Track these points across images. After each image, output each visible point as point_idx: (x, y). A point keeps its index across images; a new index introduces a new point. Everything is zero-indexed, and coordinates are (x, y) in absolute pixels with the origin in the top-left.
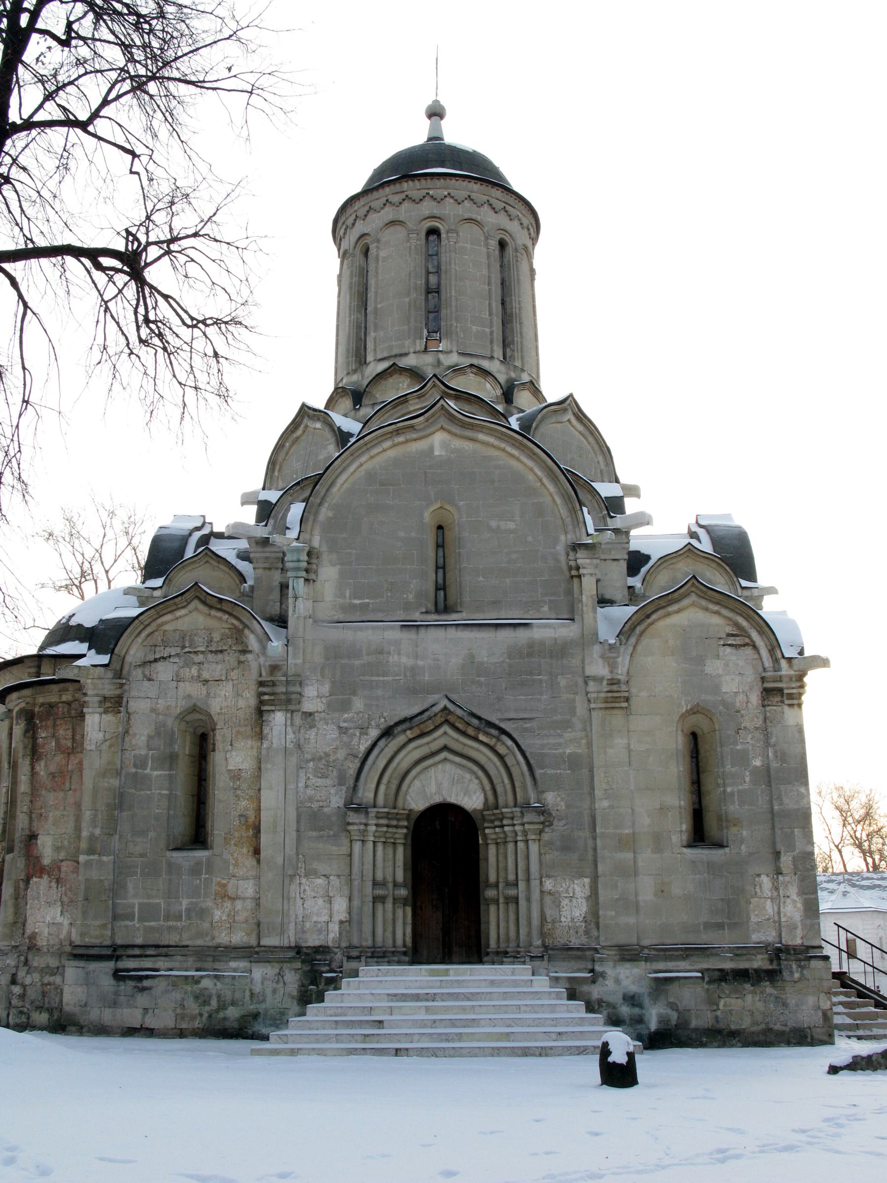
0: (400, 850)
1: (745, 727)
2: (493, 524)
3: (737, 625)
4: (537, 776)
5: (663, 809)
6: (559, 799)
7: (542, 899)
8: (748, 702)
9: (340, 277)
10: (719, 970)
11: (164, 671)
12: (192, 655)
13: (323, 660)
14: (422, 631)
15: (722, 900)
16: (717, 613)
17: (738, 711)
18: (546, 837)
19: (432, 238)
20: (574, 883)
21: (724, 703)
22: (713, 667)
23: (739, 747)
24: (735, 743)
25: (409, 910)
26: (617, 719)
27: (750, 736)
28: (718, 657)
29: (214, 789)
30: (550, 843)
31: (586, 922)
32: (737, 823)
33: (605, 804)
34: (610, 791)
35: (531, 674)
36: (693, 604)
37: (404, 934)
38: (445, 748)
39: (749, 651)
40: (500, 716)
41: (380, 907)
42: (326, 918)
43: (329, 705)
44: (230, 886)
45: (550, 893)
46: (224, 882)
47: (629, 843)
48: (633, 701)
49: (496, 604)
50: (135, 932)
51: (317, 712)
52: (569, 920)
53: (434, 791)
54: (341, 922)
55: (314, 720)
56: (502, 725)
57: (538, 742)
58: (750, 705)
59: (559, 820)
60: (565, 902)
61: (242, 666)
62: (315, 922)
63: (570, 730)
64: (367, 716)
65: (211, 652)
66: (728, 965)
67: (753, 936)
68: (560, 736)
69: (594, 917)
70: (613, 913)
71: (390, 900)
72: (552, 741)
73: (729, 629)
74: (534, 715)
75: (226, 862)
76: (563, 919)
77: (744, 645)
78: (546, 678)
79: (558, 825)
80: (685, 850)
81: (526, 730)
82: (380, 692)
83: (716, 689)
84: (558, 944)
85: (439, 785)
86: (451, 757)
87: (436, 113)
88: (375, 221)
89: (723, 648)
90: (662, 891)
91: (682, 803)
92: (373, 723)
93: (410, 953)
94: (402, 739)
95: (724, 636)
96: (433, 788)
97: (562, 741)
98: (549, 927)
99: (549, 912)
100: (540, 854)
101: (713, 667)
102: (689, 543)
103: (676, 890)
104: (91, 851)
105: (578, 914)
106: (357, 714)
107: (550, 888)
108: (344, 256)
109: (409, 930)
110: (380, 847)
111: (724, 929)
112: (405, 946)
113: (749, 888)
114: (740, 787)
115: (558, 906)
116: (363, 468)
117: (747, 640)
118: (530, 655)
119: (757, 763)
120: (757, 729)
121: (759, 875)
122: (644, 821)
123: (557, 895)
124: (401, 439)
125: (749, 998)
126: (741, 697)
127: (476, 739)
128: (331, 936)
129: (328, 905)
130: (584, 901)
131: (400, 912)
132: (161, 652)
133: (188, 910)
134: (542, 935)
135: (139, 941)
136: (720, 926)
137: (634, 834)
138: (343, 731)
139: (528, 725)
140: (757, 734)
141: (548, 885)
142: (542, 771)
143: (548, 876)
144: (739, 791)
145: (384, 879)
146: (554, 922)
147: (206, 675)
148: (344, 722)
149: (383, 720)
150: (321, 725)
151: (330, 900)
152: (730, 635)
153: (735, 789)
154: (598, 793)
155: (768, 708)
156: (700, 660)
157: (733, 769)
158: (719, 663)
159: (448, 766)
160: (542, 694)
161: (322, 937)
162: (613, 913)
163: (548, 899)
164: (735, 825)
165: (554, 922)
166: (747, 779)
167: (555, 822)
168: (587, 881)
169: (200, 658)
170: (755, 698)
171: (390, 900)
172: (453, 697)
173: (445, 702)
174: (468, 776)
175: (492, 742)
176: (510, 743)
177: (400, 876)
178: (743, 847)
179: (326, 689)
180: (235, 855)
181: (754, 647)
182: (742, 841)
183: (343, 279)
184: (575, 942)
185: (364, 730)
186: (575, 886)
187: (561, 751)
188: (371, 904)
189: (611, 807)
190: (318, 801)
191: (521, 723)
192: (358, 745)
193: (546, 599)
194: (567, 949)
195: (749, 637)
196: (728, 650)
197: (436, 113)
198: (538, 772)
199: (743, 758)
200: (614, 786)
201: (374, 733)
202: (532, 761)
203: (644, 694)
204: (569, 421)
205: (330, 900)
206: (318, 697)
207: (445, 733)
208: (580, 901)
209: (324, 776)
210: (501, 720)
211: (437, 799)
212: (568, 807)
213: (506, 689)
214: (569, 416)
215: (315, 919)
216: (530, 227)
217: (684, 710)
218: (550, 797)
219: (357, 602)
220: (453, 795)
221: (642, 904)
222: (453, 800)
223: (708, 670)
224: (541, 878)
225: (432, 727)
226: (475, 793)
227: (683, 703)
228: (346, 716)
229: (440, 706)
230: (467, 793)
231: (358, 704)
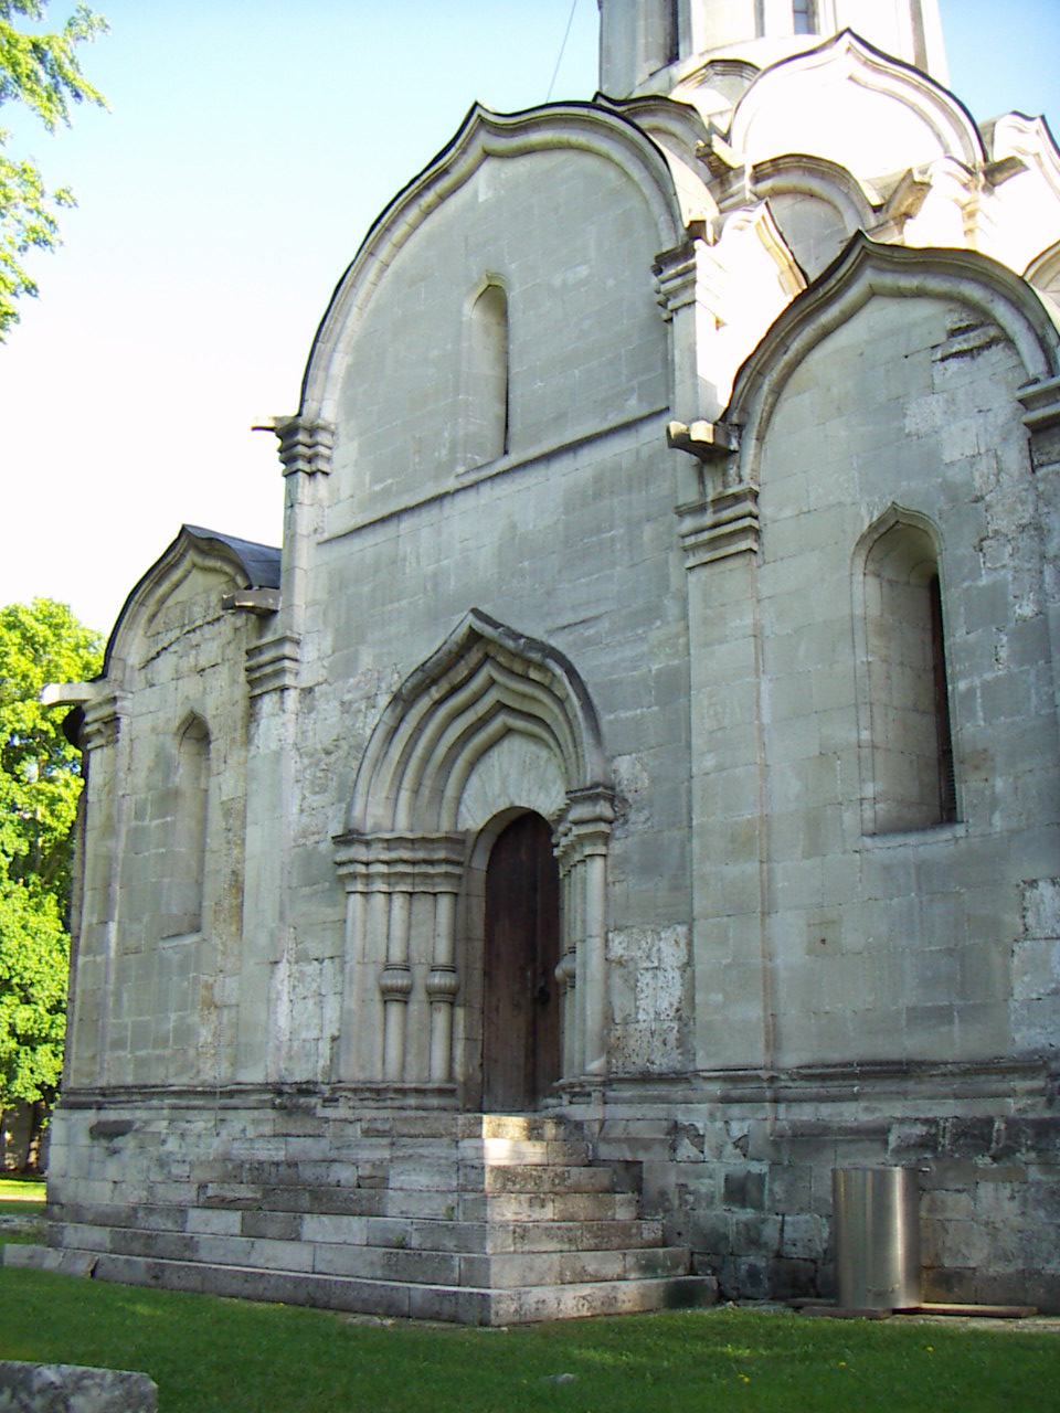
0: (445, 904)
1: (996, 532)
2: (557, 281)
3: (966, 303)
4: (604, 728)
5: (826, 756)
6: (638, 767)
7: (607, 976)
8: (1000, 471)
10: (927, 1121)
11: (165, 665)
12: (191, 635)
13: (327, 596)
14: (447, 502)
15: (950, 952)
16: (920, 294)
17: (978, 499)
18: (616, 847)
20: (660, 939)
21: (949, 490)
22: (924, 413)
23: (984, 581)
24: (975, 574)
25: (460, 1013)
26: (733, 576)
27: (1009, 549)
28: (931, 389)
30: (624, 860)
31: (680, 1019)
32: (982, 759)
33: (709, 762)
34: (719, 734)
35: (599, 530)
36: (873, 293)
37: (451, 1059)
38: (501, 707)
39: (997, 354)
40: (550, 624)
41: (395, 1010)
42: (315, 1033)
43: (331, 669)
44: (217, 990)
45: (621, 963)
46: (211, 980)
47: (750, 842)
48: (767, 537)
49: (560, 418)
50: (119, 1069)
51: (318, 684)
52: (652, 1016)
53: (497, 791)
54: (334, 1039)
55: (314, 699)
56: (553, 642)
57: (607, 659)
58: (1004, 478)
59: (639, 810)
60: (646, 979)
61: (238, 633)
62: (304, 1041)
63: (658, 623)
64: (376, 675)
65: (208, 623)
66: (947, 1110)
67: (1018, 1037)
68: (642, 639)
69: (685, 1013)
70: (720, 997)
71: (419, 996)
72: (628, 652)
73: (953, 320)
74: (602, 609)
75: (215, 949)
76: (642, 1016)
77: (988, 345)
78: (622, 531)
79: (637, 818)
80: (868, 842)
81: (588, 642)
82: (393, 630)
83: (932, 459)
84: (632, 1068)
85: (504, 780)
89: (940, 366)
90: (822, 943)
91: (865, 735)
92: (383, 685)
93: (460, 1092)
94: (424, 704)
95: (942, 338)
96: (496, 786)
97: (645, 648)
98: (618, 1033)
99: (617, 1001)
100: (606, 884)
101: (924, 413)
103: (851, 938)
104: (87, 953)
105: (666, 1005)
106: (364, 674)
107: (621, 952)
109: (459, 1051)
110: (398, 901)
111: (951, 1022)
112: (450, 1076)
113: (1012, 919)
114: (988, 676)
115: (633, 987)
116: (390, 270)
117: (993, 332)
118: (597, 496)
119: (1027, 609)
120: (1023, 528)
121: (1033, 883)
122: (788, 789)
123: (631, 966)
124: (430, 197)
125: (986, 1190)
126: (986, 465)
127: (526, 678)
128: (322, 1063)
129: (318, 1010)
130: (677, 974)
131: (441, 1019)
132: (165, 640)
133: (176, 1029)
134: (608, 1049)
135: (129, 1080)
136: (943, 1015)
137: (766, 819)
138: (346, 707)
139: (592, 631)
140: (1025, 542)
141: (618, 946)
142: (612, 717)
143: (619, 929)
144: (986, 686)
145: (408, 959)
146: (626, 1023)
147: (203, 663)
148: (349, 691)
149: (396, 676)
150: (321, 705)
151: (320, 1005)
152: (954, 333)
153: (977, 682)
154: (697, 742)
155: (1041, 473)
156: (897, 407)
157: (972, 637)
158: (935, 404)
159: (513, 745)
160: (613, 565)
161: (310, 1066)
162: (720, 997)
163: (617, 974)
164: (977, 768)
165: (626, 1023)
166: (1003, 654)
167: (633, 816)
168: (682, 929)
169: (195, 638)
170: (1014, 457)
171: (419, 996)
172: (486, 609)
173: (471, 620)
174: (544, 753)
175: (547, 682)
176: (559, 671)
177: (442, 955)
178: (997, 819)
179: (328, 643)
180: (224, 938)
181: (1009, 342)
182: (994, 803)
184: (662, 1062)
185: (371, 699)
186: (662, 944)
187: (644, 669)
188: (378, 1006)
189: (720, 768)
190: (313, 834)
191: (580, 629)
192: (363, 729)
193: (634, 383)
194: (645, 1078)
195: (995, 323)
196: (953, 364)
198: (606, 719)
199: (993, 606)
200: (726, 722)
201: (384, 700)
202: (596, 700)
203: (788, 512)
205: (320, 1005)
206: (319, 658)
207: (492, 682)
208: (670, 974)
209: (323, 790)
210: (551, 632)
211: (503, 805)
212: (653, 780)
213: (560, 572)
215: (304, 1035)
217: (866, 527)
218: (625, 767)
219: (377, 488)
220: (524, 794)
221: (783, 974)
222: (523, 802)
223: (910, 425)
224: (607, 933)
225: (466, 672)
226: (554, 783)
227: (863, 511)
228: (351, 681)
229: (464, 629)
230: (543, 786)
231: (366, 659)
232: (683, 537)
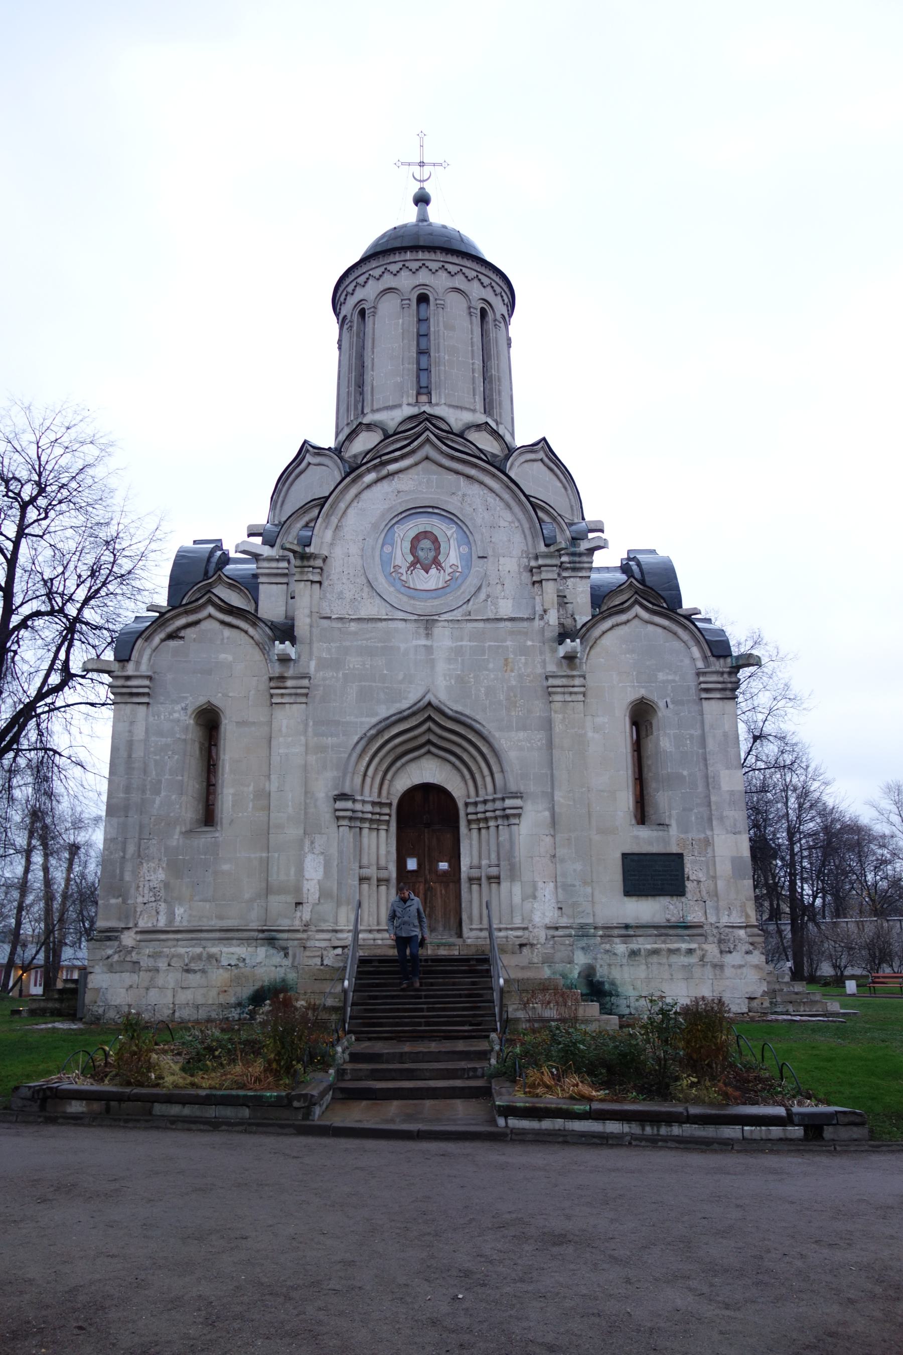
9: (340, 342)
19: (423, 306)
29: (223, 787)
38: (429, 742)
86: (433, 750)
87: (422, 199)
88: (369, 292)
102: (487, 423)
108: (342, 322)
174: (448, 767)
183: (343, 343)
197: (422, 199)
204: (542, 460)
207: (429, 730)
214: (541, 455)
216: (503, 294)
232: (548, 687)
